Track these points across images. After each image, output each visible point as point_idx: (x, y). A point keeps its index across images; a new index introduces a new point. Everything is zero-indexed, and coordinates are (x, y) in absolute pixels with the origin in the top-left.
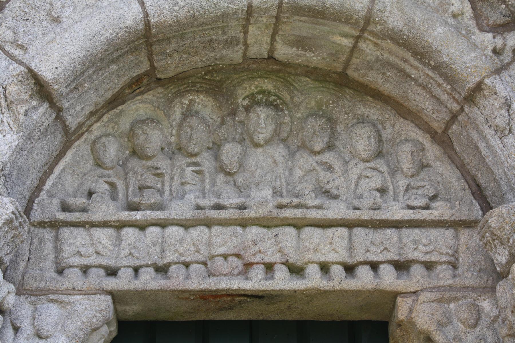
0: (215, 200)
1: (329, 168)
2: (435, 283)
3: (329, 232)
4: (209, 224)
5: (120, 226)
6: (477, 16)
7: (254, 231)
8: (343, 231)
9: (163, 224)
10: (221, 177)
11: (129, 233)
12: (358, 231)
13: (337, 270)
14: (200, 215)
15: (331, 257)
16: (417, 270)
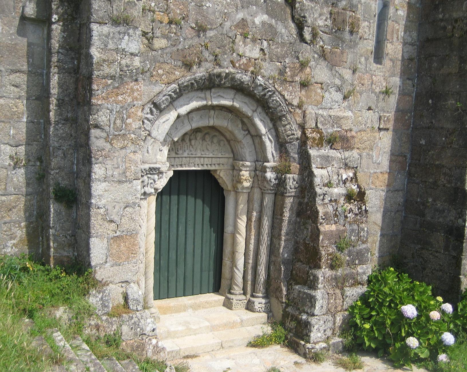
0: (191, 153)
1: (209, 145)
2: (224, 168)
3: (209, 159)
4: (190, 157)
5: (175, 158)
6: (242, 128)
7: (197, 159)
8: (211, 159)
9: (182, 157)
10: (191, 146)
11: (177, 159)
12: (213, 159)
13: (209, 166)
14: (189, 156)
15: (208, 163)
16: (221, 165)
